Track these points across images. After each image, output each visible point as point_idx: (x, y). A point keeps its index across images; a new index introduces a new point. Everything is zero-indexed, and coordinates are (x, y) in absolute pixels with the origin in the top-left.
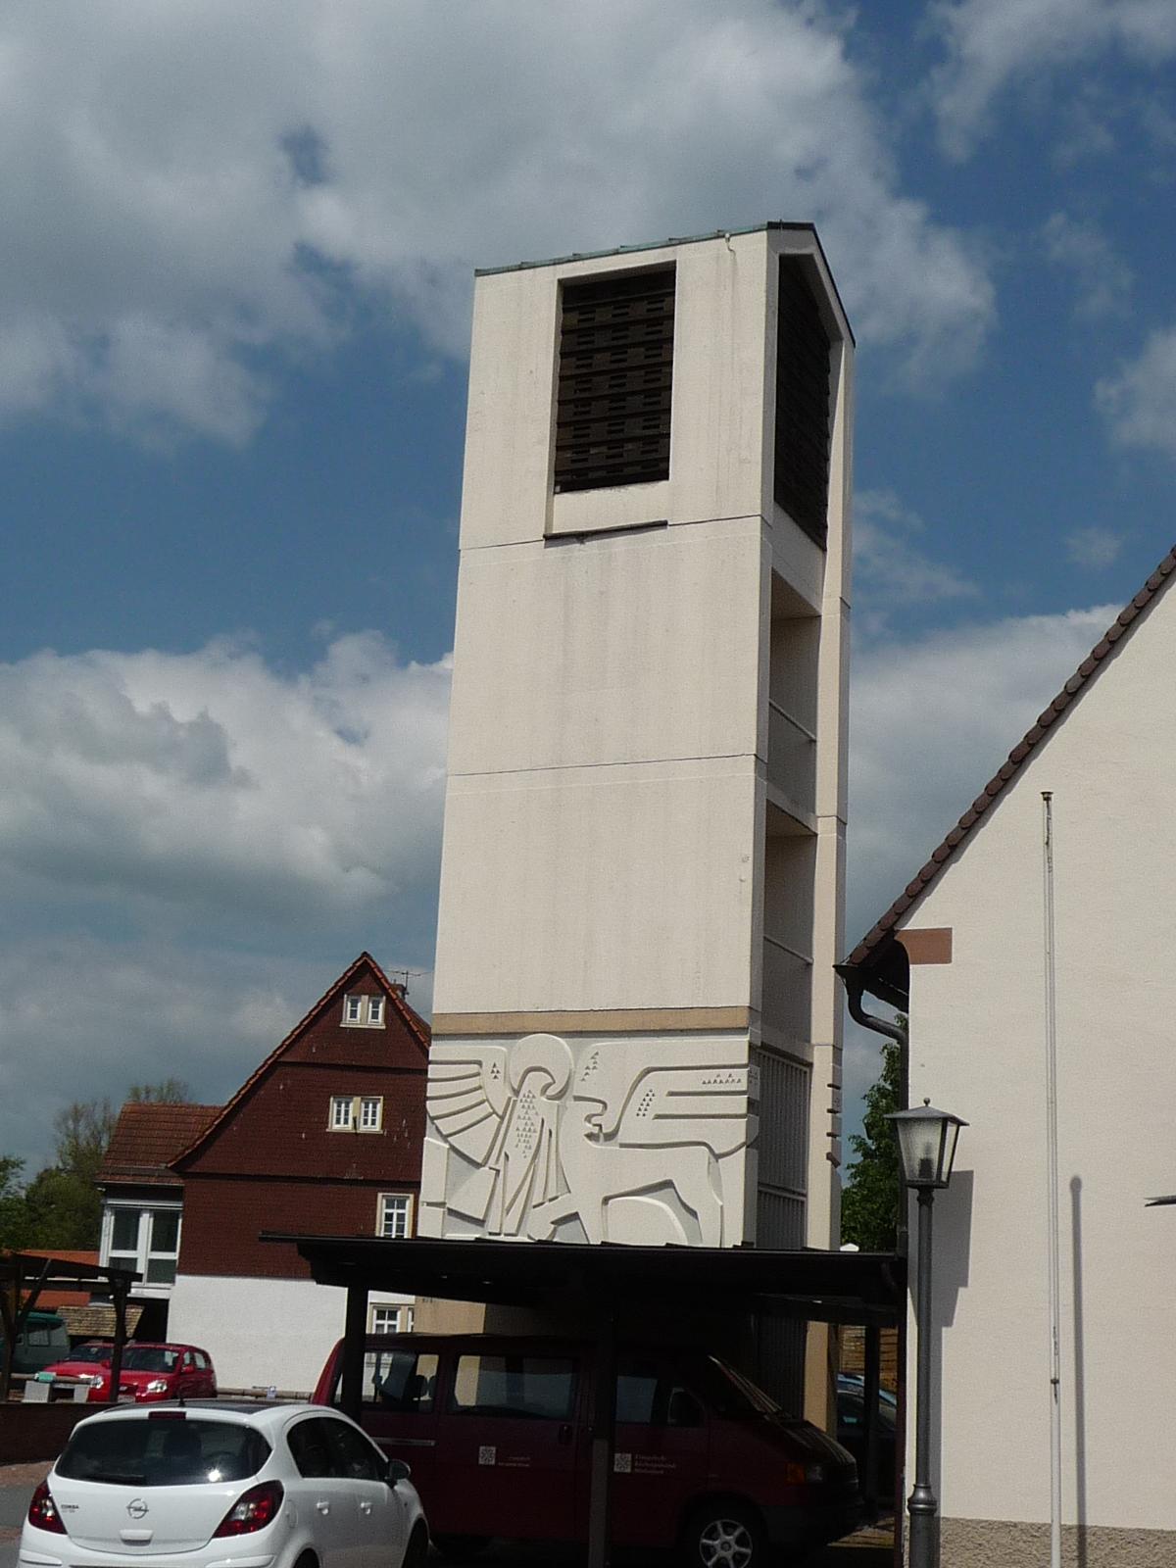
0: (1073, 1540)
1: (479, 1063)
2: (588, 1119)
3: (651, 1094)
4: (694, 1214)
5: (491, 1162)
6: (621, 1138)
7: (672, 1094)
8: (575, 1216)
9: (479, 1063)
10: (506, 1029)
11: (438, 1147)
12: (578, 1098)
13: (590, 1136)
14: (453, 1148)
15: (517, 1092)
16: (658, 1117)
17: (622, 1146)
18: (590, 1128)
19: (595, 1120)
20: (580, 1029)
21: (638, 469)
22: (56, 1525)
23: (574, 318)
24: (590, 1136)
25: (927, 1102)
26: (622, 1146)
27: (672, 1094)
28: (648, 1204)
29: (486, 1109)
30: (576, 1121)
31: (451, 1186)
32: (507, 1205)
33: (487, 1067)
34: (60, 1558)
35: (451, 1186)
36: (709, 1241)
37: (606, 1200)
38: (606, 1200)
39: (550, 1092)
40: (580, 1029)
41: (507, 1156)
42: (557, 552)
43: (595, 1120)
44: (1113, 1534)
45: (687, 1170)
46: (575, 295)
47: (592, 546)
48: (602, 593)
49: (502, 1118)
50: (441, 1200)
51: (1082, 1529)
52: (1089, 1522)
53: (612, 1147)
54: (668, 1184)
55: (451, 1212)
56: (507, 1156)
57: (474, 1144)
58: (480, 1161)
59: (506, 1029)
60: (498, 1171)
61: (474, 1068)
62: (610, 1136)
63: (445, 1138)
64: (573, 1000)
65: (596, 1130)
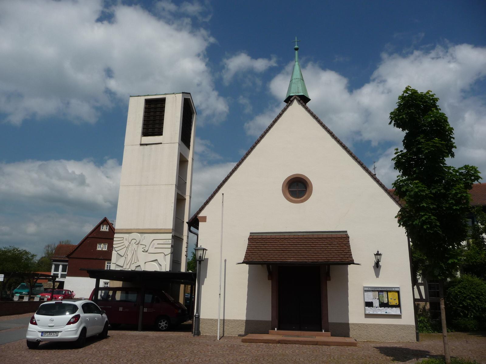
0: (222, 321)
1: (123, 238)
2: (143, 248)
3: (154, 244)
4: (161, 265)
5: (125, 256)
6: (149, 252)
7: (158, 244)
8: (139, 266)
9: (123, 238)
10: (129, 232)
11: (115, 253)
12: (141, 245)
13: (143, 251)
14: (118, 253)
15: (130, 243)
16: (155, 248)
17: (149, 253)
18: (143, 250)
19: (144, 248)
20: (142, 232)
21: (157, 133)
22: (35, 324)
23: (147, 106)
24: (143, 251)
25: (201, 246)
26: (149, 253)
27: (158, 244)
28: (153, 264)
29: (124, 246)
30: (140, 249)
31: (117, 260)
32: (127, 263)
33: (125, 239)
34: (35, 330)
35: (117, 260)
36: (163, 270)
37: (145, 263)
38: (145, 263)
39: (136, 243)
40: (142, 232)
41: (128, 255)
42: (142, 147)
43: (144, 248)
44: (229, 320)
45: (160, 257)
46: (147, 102)
47: (148, 146)
48: (150, 155)
49: (127, 248)
50: (115, 263)
51: (224, 320)
52: (225, 319)
53: (147, 253)
54: (156, 260)
55: (117, 265)
56: (128, 255)
57: (122, 253)
58: (122, 255)
59: (129, 232)
60: (126, 258)
61: (122, 239)
62: (147, 251)
63: (116, 251)
64: (141, 227)
65: (144, 250)
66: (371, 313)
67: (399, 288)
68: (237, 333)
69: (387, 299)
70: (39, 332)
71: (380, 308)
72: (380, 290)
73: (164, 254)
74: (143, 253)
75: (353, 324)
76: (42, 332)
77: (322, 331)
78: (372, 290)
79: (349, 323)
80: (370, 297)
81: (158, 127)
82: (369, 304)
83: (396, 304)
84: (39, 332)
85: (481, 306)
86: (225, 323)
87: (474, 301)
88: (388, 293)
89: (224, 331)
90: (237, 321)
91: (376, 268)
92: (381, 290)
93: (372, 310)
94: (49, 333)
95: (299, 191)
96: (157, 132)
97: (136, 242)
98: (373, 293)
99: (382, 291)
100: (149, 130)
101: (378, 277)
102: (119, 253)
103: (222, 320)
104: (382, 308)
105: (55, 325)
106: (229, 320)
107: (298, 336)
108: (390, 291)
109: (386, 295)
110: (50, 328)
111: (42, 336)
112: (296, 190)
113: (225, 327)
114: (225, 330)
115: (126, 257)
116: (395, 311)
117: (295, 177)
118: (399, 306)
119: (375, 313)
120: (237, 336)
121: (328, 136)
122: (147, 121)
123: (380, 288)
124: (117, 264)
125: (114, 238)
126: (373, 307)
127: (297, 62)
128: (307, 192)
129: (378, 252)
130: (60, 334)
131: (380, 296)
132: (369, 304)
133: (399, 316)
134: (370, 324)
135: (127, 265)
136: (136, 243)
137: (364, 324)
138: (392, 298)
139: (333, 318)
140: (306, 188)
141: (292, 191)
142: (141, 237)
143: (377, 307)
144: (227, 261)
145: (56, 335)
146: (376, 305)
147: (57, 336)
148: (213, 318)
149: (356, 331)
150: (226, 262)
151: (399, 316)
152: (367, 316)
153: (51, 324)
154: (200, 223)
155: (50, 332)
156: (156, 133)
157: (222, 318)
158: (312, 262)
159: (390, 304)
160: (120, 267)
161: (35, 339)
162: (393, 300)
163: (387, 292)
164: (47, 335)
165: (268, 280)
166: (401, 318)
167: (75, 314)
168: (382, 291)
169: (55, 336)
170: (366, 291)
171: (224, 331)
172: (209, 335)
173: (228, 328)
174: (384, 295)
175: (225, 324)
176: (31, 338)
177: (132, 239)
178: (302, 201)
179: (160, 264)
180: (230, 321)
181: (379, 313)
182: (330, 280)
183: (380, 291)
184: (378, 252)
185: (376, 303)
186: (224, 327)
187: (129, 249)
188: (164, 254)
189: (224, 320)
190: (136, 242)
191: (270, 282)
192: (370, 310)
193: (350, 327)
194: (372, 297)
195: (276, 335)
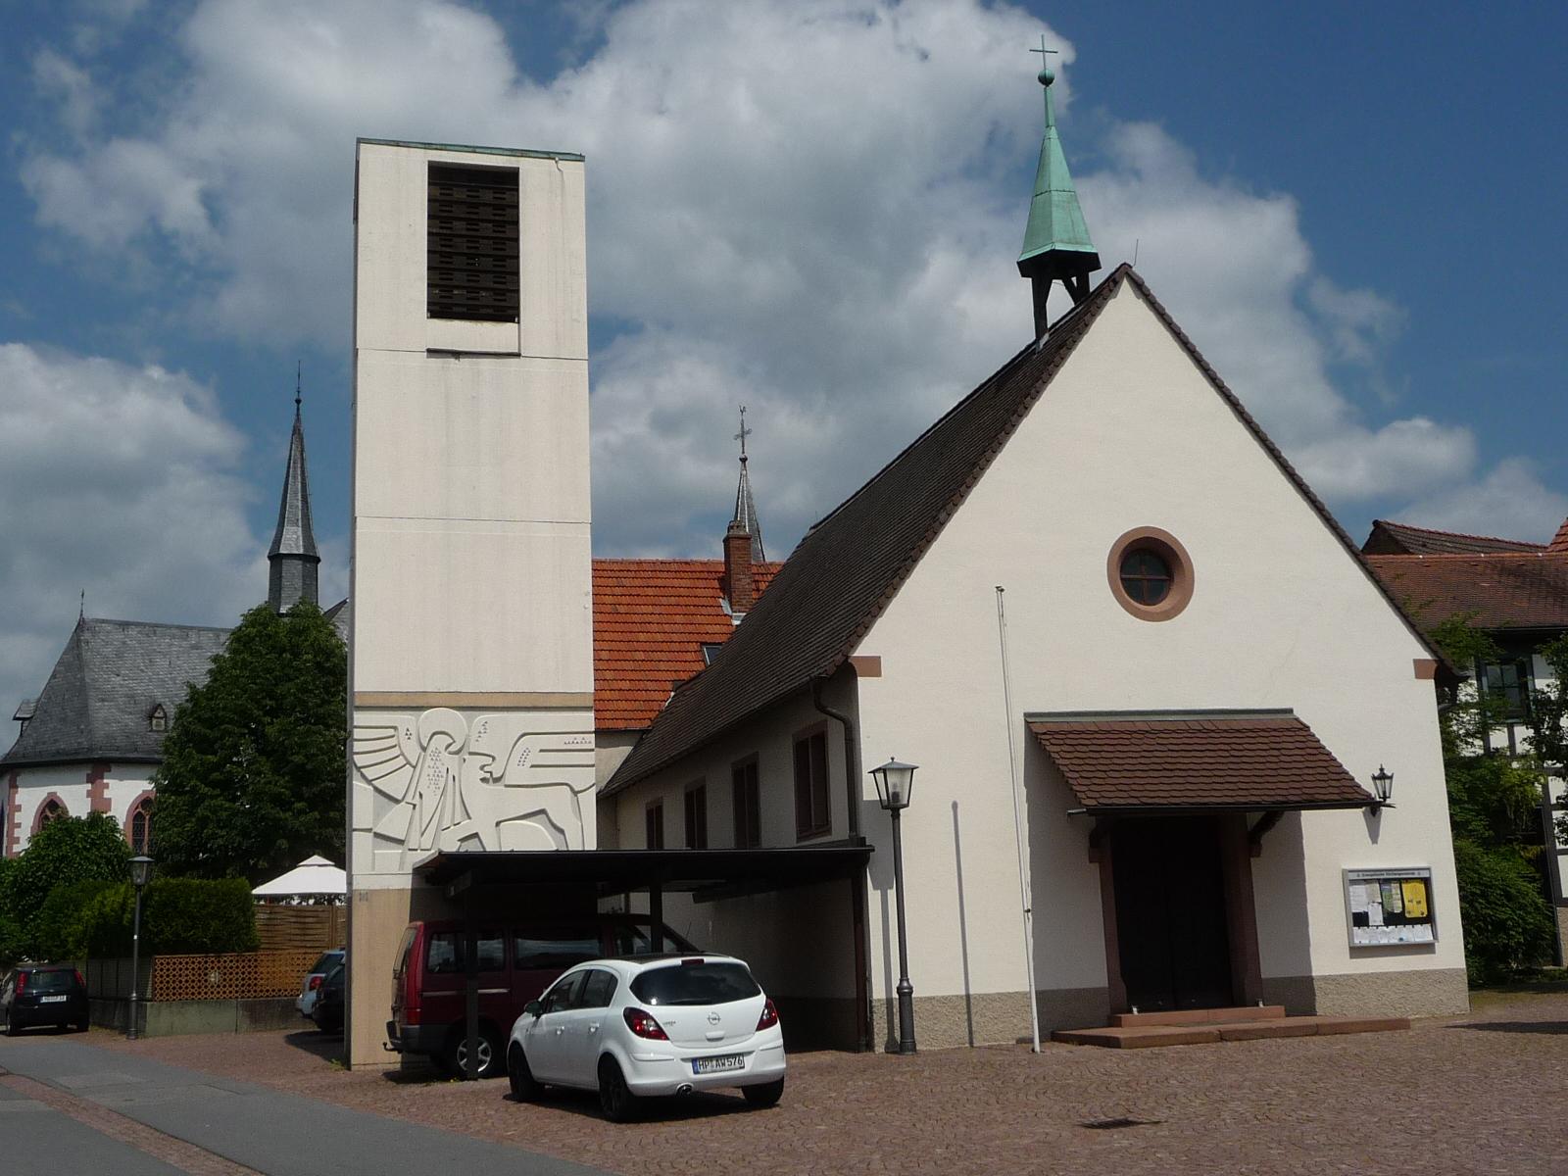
0: (964, 1003)
1: (395, 728)
2: (482, 768)
3: (527, 751)
4: (562, 831)
5: (409, 799)
6: (507, 780)
7: (541, 751)
8: (476, 835)
9: (395, 728)
10: (415, 705)
11: (365, 789)
12: (471, 754)
13: (484, 780)
14: (377, 789)
15: (424, 749)
16: (532, 766)
17: (506, 786)
18: (483, 775)
19: (486, 769)
20: (471, 705)
21: (490, 311)
22: (659, 1034)
23: (437, 192)
24: (484, 780)
25: (892, 759)
26: (506, 786)
27: (541, 751)
28: (529, 826)
29: (401, 761)
30: (472, 770)
31: (378, 815)
32: (423, 828)
33: (402, 731)
34: (670, 1054)
35: (378, 815)
36: (575, 845)
37: (498, 824)
38: (498, 824)
39: (451, 749)
40: (471, 705)
41: (421, 795)
42: (437, 362)
43: (486, 769)
44: (984, 997)
45: (558, 804)
46: (440, 174)
47: (465, 361)
48: (474, 397)
49: (414, 767)
50: (369, 827)
51: (968, 996)
52: (971, 992)
53: (499, 787)
54: (543, 812)
55: (377, 835)
56: (421, 795)
57: (394, 786)
58: (400, 798)
59: (415, 705)
60: (415, 806)
61: (391, 732)
62: (497, 780)
63: (370, 782)
64: (466, 685)
65: (488, 775)
66: (1365, 942)
67: (1429, 869)
68: (1013, 1035)
69: (1400, 902)
70: (684, 1060)
71: (1385, 928)
72: (1385, 877)
73: (572, 789)
74: (484, 785)
75: (1324, 978)
76: (694, 1060)
77: (1258, 1005)
78: (1365, 880)
79: (1311, 979)
80: (1364, 899)
81: (492, 285)
82: (1361, 920)
83: (1409, 912)
84: (684, 1060)
85: (1490, 916)
86: (972, 1008)
87: (1477, 904)
88: (1403, 885)
89: (971, 1032)
90: (1009, 995)
91: (1371, 816)
92: (1388, 877)
93: (1367, 935)
94: (714, 1063)
95: (1148, 580)
96: (488, 307)
97: (450, 745)
98: (1367, 886)
99: (1388, 881)
100: (456, 292)
101: (1377, 843)
102: (381, 787)
103: (961, 997)
104: (1391, 927)
105: (727, 1035)
106: (985, 994)
107: (1199, 1024)
108: (1407, 880)
109: (1399, 892)
110: (714, 1044)
111: (696, 1072)
112: (1139, 577)
113: (975, 1019)
114: (973, 1029)
115: (417, 801)
116: (1420, 934)
117: (1169, 543)
118: (1429, 919)
119: (1374, 942)
120: (1014, 1042)
121: (1227, 410)
122: (442, 254)
123: (1416, 872)
124: (375, 830)
125: (595, 732)
126: (1368, 926)
127: (1053, 128)
128: (1172, 593)
129: (1382, 770)
130: (748, 1061)
131: (1384, 894)
132: (1361, 920)
133: (1427, 948)
134: (1365, 975)
135: (422, 834)
136: (452, 749)
137: (1348, 976)
138: (1412, 899)
139: (1271, 967)
140: (1170, 578)
141: (1129, 579)
142: (469, 727)
143: (1377, 927)
144: (959, 806)
145: (737, 1065)
146: (1375, 921)
147: (741, 1068)
148: (933, 995)
149: (1330, 996)
150: (959, 810)
151: (1427, 948)
152: (1357, 951)
153: (716, 1030)
154: (861, 681)
155: (718, 1058)
156: (455, 309)
157: (963, 993)
158: (1274, 803)
159: (1407, 915)
160: (393, 845)
161: (671, 1086)
162: (1415, 903)
163: (1400, 881)
164: (712, 1066)
165: (1091, 862)
166: (1434, 952)
167: (641, 1008)
168: (1388, 881)
169: (736, 1069)
170: (1354, 882)
171: (971, 1032)
172: (928, 1048)
173: (984, 1019)
174: (1394, 891)
175: (973, 1010)
176: (653, 1084)
177: (434, 734)
178: (1167, 616)
179: (559, 825)
180: (985, 998)
181: (1384, 941)
182: (1259, 856)
183: (1385, 880)
184: (1382, 770)
185: (1376, 916)
186: (969, 1020)
187: (426, 771)
188: (572, 789)
189: (968, 996)
190: (450, 745)
191: (1095, 867)
192: (1363, 936)
193: (1316, 987)
194: (1365, 899)
195: (1137, 1023)
